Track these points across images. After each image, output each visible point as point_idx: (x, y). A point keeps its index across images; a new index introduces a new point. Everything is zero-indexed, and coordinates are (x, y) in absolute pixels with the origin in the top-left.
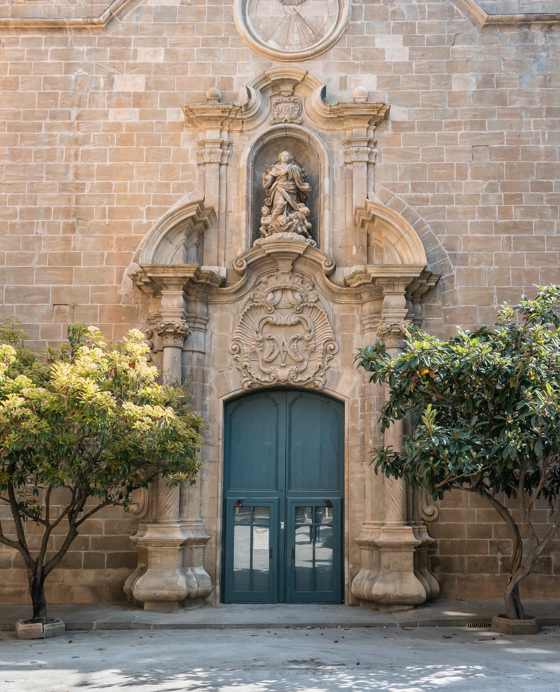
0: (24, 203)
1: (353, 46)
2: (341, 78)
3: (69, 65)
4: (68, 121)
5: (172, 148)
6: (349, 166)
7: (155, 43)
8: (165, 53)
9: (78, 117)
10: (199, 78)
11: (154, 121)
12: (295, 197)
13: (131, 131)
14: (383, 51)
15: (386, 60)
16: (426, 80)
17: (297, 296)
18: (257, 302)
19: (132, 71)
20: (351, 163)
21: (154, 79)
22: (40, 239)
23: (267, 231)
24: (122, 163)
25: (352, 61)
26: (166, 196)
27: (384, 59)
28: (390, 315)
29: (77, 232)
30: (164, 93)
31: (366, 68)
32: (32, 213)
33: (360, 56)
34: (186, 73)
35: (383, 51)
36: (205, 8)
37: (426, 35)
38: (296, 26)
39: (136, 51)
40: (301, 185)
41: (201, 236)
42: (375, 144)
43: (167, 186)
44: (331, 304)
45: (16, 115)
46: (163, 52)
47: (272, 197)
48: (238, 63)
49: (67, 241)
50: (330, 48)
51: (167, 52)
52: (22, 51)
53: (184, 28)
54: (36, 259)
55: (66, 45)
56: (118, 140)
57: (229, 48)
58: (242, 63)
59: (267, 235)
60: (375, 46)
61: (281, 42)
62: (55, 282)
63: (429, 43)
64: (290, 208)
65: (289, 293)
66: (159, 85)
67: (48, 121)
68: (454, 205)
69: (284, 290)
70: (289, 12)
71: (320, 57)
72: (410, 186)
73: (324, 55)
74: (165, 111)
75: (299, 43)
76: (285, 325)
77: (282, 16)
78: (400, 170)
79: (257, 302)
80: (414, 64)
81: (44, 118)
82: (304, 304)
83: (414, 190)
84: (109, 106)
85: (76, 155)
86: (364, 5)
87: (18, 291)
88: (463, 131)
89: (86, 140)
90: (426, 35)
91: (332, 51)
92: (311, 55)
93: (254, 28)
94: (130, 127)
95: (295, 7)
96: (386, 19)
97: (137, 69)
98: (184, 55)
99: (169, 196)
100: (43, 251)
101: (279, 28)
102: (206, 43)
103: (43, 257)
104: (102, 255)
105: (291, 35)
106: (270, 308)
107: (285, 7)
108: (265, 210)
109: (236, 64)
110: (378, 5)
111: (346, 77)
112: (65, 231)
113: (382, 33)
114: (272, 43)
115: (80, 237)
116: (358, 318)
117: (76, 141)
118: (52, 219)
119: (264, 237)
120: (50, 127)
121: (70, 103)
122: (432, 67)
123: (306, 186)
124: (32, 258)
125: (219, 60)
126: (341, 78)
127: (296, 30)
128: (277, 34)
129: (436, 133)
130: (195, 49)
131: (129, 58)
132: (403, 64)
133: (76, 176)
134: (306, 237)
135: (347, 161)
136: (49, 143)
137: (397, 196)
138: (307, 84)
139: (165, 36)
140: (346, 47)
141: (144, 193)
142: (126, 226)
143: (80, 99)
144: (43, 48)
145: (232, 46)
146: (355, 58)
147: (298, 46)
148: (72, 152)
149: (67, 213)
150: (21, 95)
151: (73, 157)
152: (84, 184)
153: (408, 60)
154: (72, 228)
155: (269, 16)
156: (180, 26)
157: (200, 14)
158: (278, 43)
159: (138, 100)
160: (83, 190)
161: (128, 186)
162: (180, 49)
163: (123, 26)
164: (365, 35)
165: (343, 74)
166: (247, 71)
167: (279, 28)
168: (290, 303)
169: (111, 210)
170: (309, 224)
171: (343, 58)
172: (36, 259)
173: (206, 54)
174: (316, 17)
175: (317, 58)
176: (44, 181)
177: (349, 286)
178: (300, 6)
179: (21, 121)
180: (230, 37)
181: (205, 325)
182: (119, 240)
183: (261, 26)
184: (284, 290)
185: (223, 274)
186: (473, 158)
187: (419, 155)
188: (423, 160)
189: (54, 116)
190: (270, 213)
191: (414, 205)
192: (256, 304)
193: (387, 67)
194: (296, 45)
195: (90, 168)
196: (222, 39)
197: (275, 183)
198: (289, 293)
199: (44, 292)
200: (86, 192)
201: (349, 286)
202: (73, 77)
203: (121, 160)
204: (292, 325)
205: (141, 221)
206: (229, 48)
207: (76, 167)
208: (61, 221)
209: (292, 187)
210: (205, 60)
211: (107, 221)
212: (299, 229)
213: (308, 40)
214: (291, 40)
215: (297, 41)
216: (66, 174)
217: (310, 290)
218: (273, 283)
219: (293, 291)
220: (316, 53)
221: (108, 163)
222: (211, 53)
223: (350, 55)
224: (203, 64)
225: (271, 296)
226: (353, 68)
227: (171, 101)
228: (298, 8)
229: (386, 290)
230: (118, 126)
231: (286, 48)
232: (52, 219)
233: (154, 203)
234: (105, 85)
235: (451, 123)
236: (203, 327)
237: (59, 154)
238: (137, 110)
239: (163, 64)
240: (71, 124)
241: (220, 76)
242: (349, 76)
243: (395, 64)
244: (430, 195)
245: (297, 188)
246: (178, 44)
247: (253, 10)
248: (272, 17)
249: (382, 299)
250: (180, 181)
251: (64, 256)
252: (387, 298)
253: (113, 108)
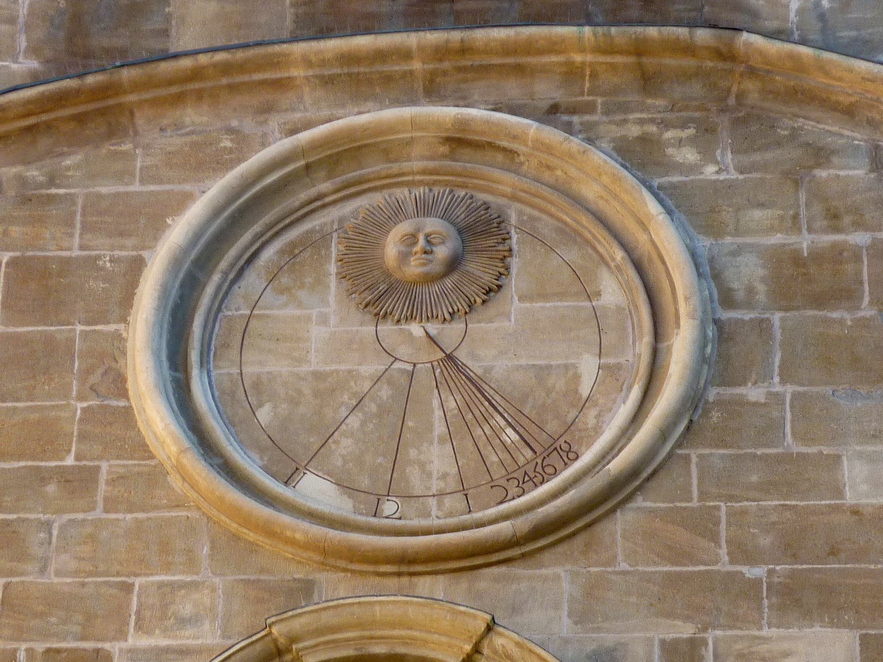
1: (731, 498)
25: (724, 565)
33: (765, 541)
38: (438, 413)
48: (138, 582)
50: (613, 510)
57: (98, 513)
58: (161, 585)
60: (838, 492)
61: (364, 482)
70: (403, 351)
71: (560, 549)
73: (580, 540)
75: (453, 484)
77: (371, 368)
91: (621, 525)
92: (513, 542)
101: (354, 421)
105: (413, 453)
109: (127, 588)
114: (315, 490)
125: (43, 571)
127: (439, 428)
128: (344, 446)
140: (695, 503)
145: (111, 505)
146: (743, 553)
147: (448, 501)
155: (305, 368)
158: (346, 487)
171: (680, 555)
175: (547, 556)
180: (104, 466)
194: (441, 495)
206: (98, 513)
213: (498, 473)
214: (414, 476)
215: (444, 476)
220: (538, 532)
223: (714, 537)
231: (389, 507)
241: (40, 647)
247: (226, 346)
248: (318, 376)
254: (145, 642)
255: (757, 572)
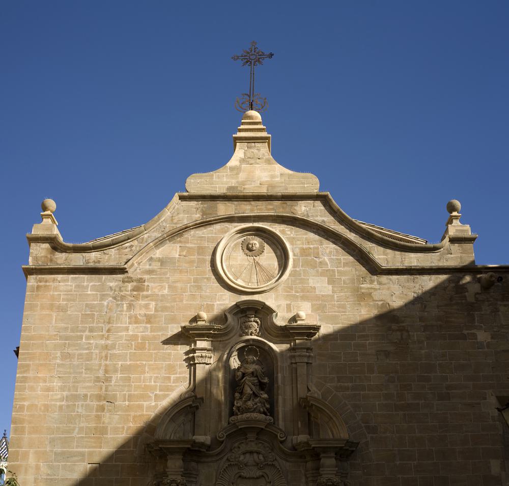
0: (69, 390)
2: (287, 305)
3: (104, 295)
4: (101, 333)
5: (172, 352)
6: (294, 365)
7: (161, 280)
8: (168, 288)
9: (109, 331)
10: (191, 304)
11: (160, 333)
12: (258, 387)
13: (144, 340)
14: (315, 288)
15: (317, 293)
16: (344, 307)
17: (261, 457)
18: (232, 461)
19: (146, 299)
20: (296, 363)
21: (161, 305)
22: (80, 416)
23: (239, 410)
24: (138, 362)
25: (294, 293)
26: (169, 385)
27: (315, 292)
28: (325, 472)
29: (106, 411)
30: (166, 315)
31: (304, 298)
32: (76, 397)
34: (182, 301)
35: (315, 288)
36: (195, 258)
37: (343, 278)
39: (148, 286)
40: (262, 379)
41: (194, 414)
42: (311, 349)
43: (169, 378)
44: (284, 462)
45: (66, 329)
46: (167, 286)
47: (242, 386)
49: (98, 418)
51: (170, 287)
52: (71, 286)
53: (181, 272)
54: (77, 430)
55: (101, 282)
56: (135, 346)
59: (239, 413)
62: (89, 448)
63: (344, 283)
64: (255, 395)
65: (255, 455)
66: (164, 309)
67: (87, 333)
68: (367, 392)
69: (251, 453)
70: (251, 261)
72: (336, 379)
74: (168, 327)
76: (253, 478)
77: (247, 263)
78: (329, 367)
79: (232, 461)
80: (335, 296)
81: (84, 331)
82: (266, 463)
83: (339, 381)
84: (129, 323)
85: (106, 357)
86: (301, 258)
87: (63, 453)
88: (371, 341)
89: (113, 347)
90: (343, 278)
93: (228, 271)
94: (143, 338)
95: (254, 257)
96: (316, 267)
97: (149, 298)
98: (181, 289)
99: (171, 386)
100: (82, 425)
101: (245, 271)
102: (196, 281)
103: (81, 429)
104: (123, 428)
106: (242, 466)
107: (248, 257)
108: (237, 395)
110: (310, 258)
111: (290, 304)
112: (97, 411)
113: (314, 276)
114: (240, 282)
115: (108, 415)
116: (303, 472)
117: (106, 347)
118: (88, 402)
119: (237, 415)
120: (88, 338)
121: (102, 321)
122: (348, 298)
123: (266, 380)
124: (74, 429)
126: (287, 305)
129: (353, 342)
130: (189, 285)
131: (143, 290)
132: (328, 296)
133: (106, 371)
134: (266, 415)
135: (293, 362)
136: (88, 349)
137: (328, 385)
138: (264, 310)
139: (168, 276)
141: (153, 383)
142: (140, 407)
143: (110, 318)
144: (85, 284)
148: (104, 354)
149: (99, 398)
150: (70, 315)
151: (103, 358)
152: (112, 377)
153: (331, 293)
154: (102, 408)
155: (237, 263)
156: (178, 270)
157: (191, 262)
159: (149, 319)
160: (110, 381)
161: (142, 378)
162: (179, 285)
163: (140, 270)
164: (302, 277)
165: (289, 302)
166: (223, 300)
167: (245, 271)
168: (255, 462)
169: (130, 396)
170: (268, 406)
172: (77, 430)
173: (196, 288)
174: (269, 265)
176: (84, 375)
177: (296, 450)
178: (258, 257)
179: (69, 333)
181: (196, 478)
182: (135, 417)
183: (233, 270)
184: (251, 453)
185: (208, 442)
186: (378, 359)
187: (341, 357)
188: (344, 361)
189: (91, 330)
190: (241, 398)
191: (340, 392)
192: (232, 463)
193: (318, 298)
195: (117, 365)
196: (207, 279)
197: (245, 378)
198: (255, 455)
199: (82, 454)
200: (113, 383)
201: (296, 450)
202: (106, 303)
203: (137, 361)
204: (257, 478)
205: (151, 404)
207: (106, 365)
208: (95, 403)
209: (256, 381)
210: (195, 292)
211: (127, 403)
212: (262, 410)
214: (253, 280)
216: (98, 370)
217: (270, 453)
218: (244, 448)
219: (258, 453)
221: (128, 363)
222: (199, 288)
224: (194, 295)
225: (242, 458)
226: (295, 298)
227: (173, 320)
228: (257, 259)
229: (322, 455)
230: (134, 337)
231: (250, 284)
232: (88, 402)
233: (160, 390)
234: (127, 309)
235: (362, 335)
236: (194, 480)
237: (94, 356)
238: (149, 326)
239: (167, 295)
240: (103, 335)
242: (292, 303)
243: (322, 296)
244: (350, 384)
245: (259, 381)
246: (177, 282)
248: (240, 264)
249: (320, 459)
250: (178, 375)
251: (96, 428)
252: (322, 461)
253: (132, 324)
254: (218, 303)
255: (297, 294)
